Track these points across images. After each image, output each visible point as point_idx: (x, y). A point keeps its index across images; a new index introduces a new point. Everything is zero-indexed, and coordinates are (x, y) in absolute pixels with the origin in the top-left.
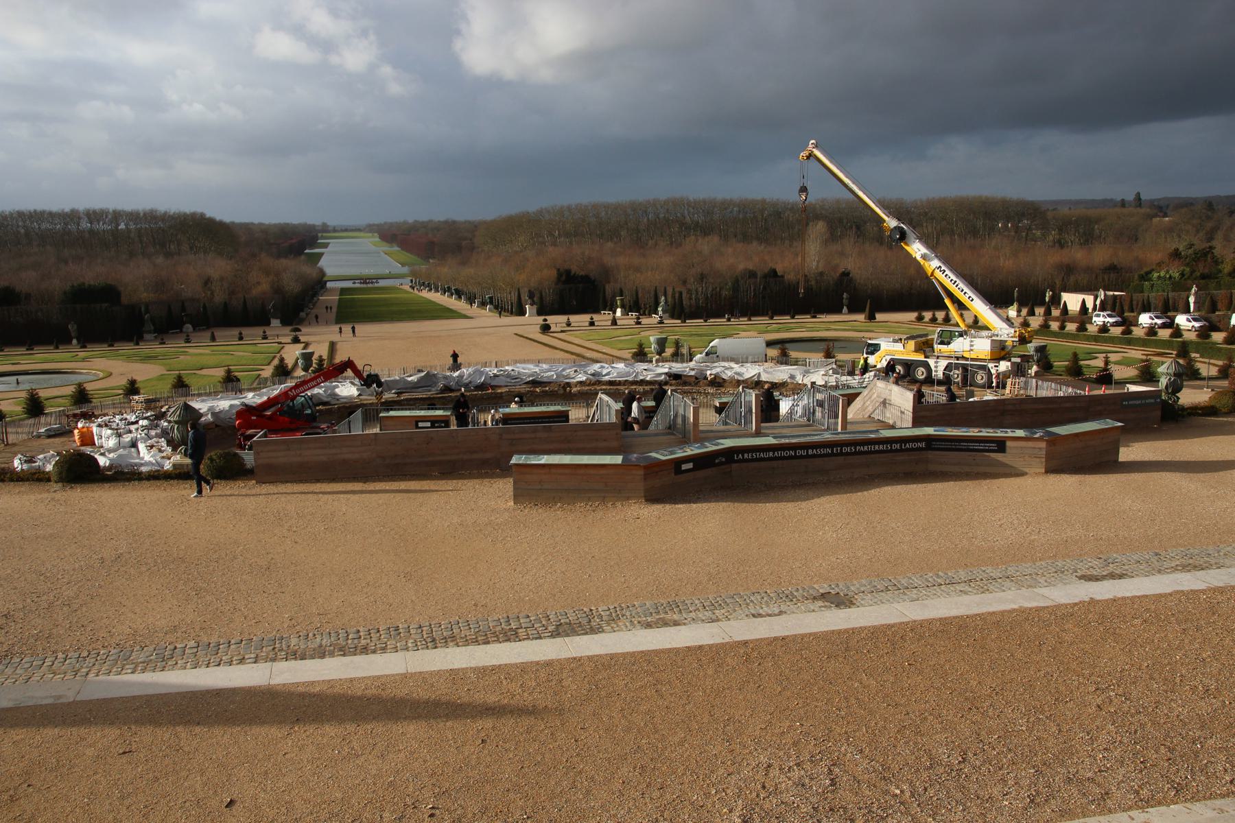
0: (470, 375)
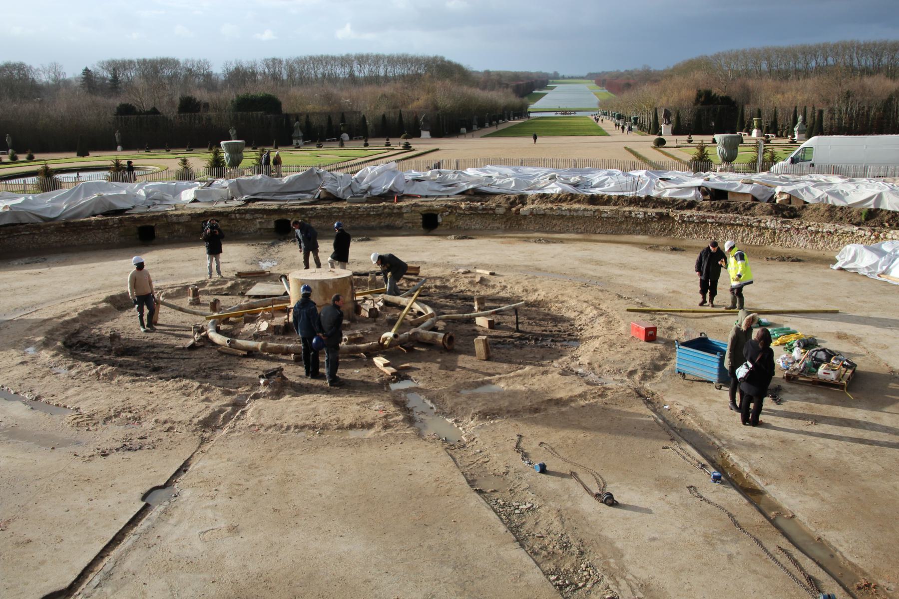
0: (373, 177)
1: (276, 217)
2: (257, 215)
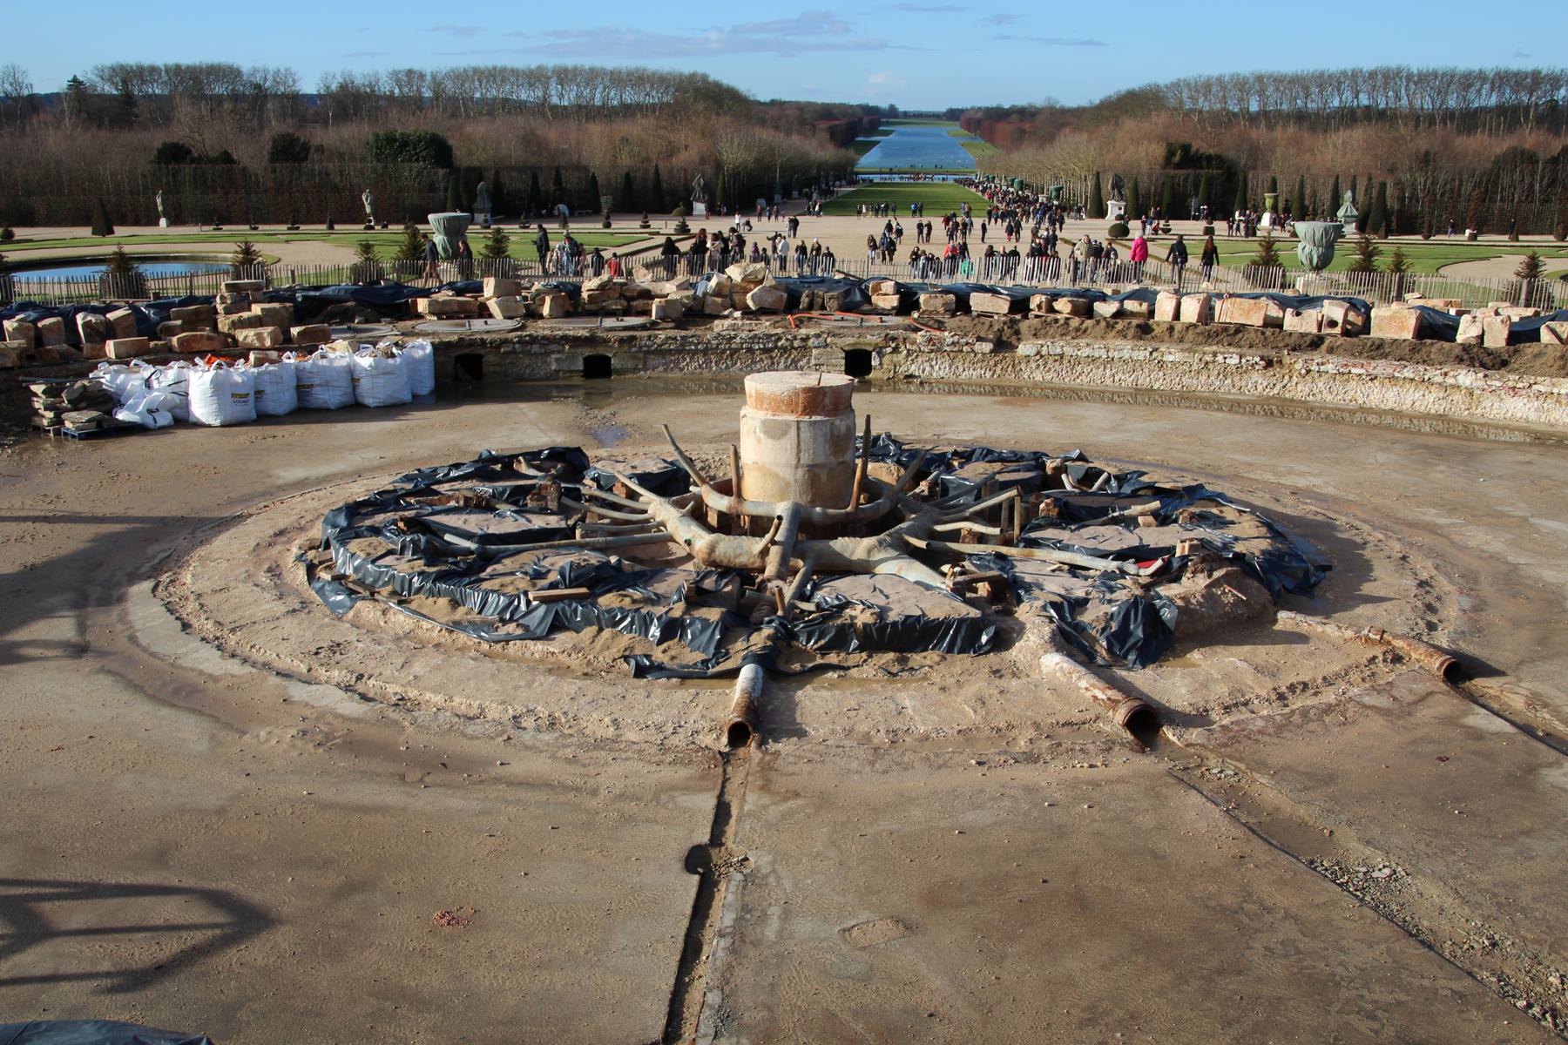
1: (588, 352)
2: (553, 347)
